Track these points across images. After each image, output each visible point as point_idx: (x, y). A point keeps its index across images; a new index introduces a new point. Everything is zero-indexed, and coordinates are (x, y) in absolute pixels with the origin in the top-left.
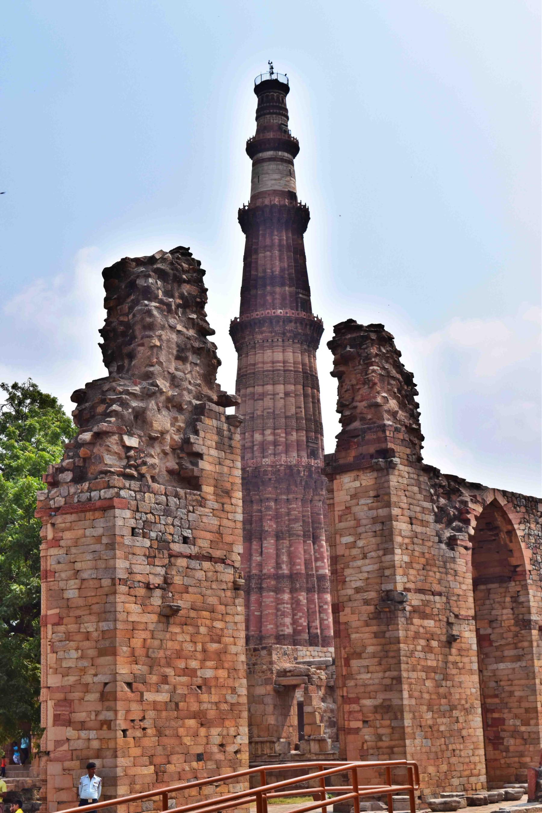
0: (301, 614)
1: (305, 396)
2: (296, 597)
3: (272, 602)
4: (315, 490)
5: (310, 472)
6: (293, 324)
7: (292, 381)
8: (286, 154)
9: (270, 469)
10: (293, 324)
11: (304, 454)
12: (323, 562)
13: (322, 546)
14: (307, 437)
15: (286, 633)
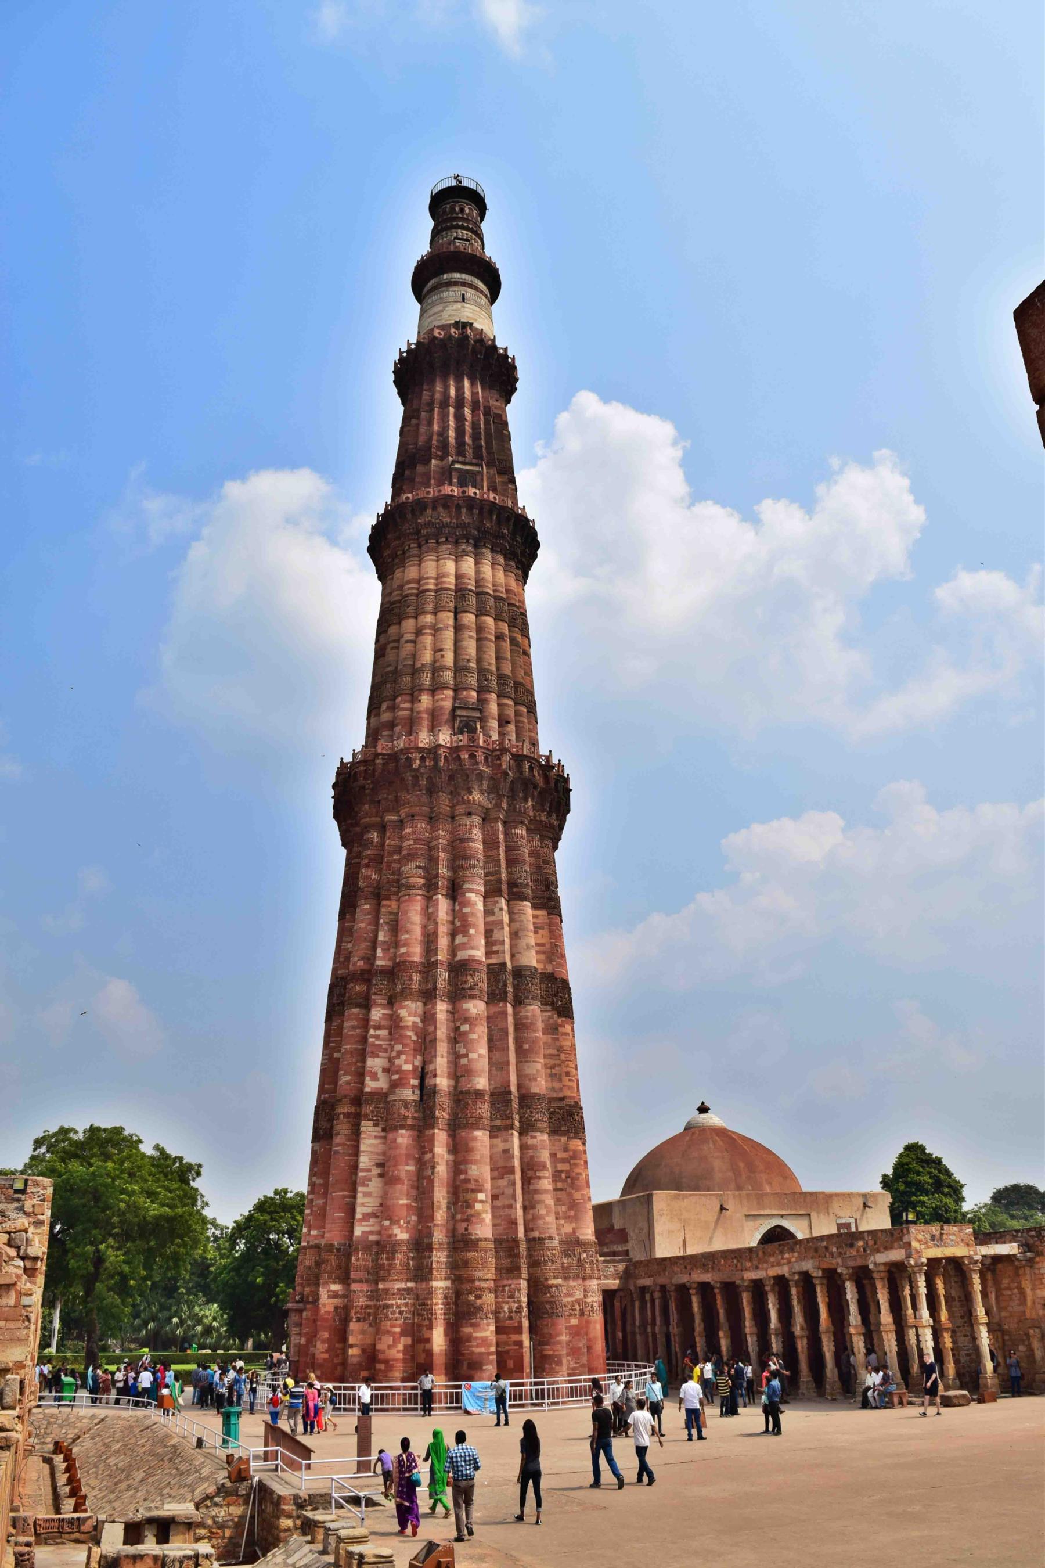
0: (398, 1047)
1: (458, 628)
2: (396, 1012)
3: (353, 1028)
5: (436, 759)
7: (430, 607)
8: (457, 276)
10: (429, 511)
12: (465, 933)
13: (467, 903)
14: (455, 699)
15: (367, 1090)
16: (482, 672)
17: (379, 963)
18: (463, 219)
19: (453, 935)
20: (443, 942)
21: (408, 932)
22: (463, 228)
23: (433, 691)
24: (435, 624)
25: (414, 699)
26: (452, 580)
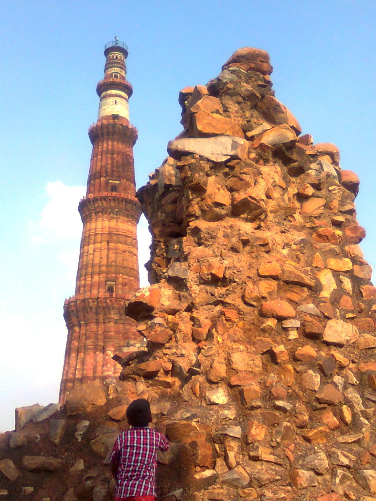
1: (109, 249)
4: (105, 314)
6: (99, 202)
9: (73, 304)
10: (99, 202)
11: (102, 290)
12: (106, 366)
14: (107, 277)
16: (116, 266)
17: (77, 376)
18: (117, 63)
19: (103, 366)
20: (99, 369)
21: (87, 365)
22: (117, 67)
23: (99, 274)
24: (100, 248)
25: (92, 277)
26: (107, 229)
